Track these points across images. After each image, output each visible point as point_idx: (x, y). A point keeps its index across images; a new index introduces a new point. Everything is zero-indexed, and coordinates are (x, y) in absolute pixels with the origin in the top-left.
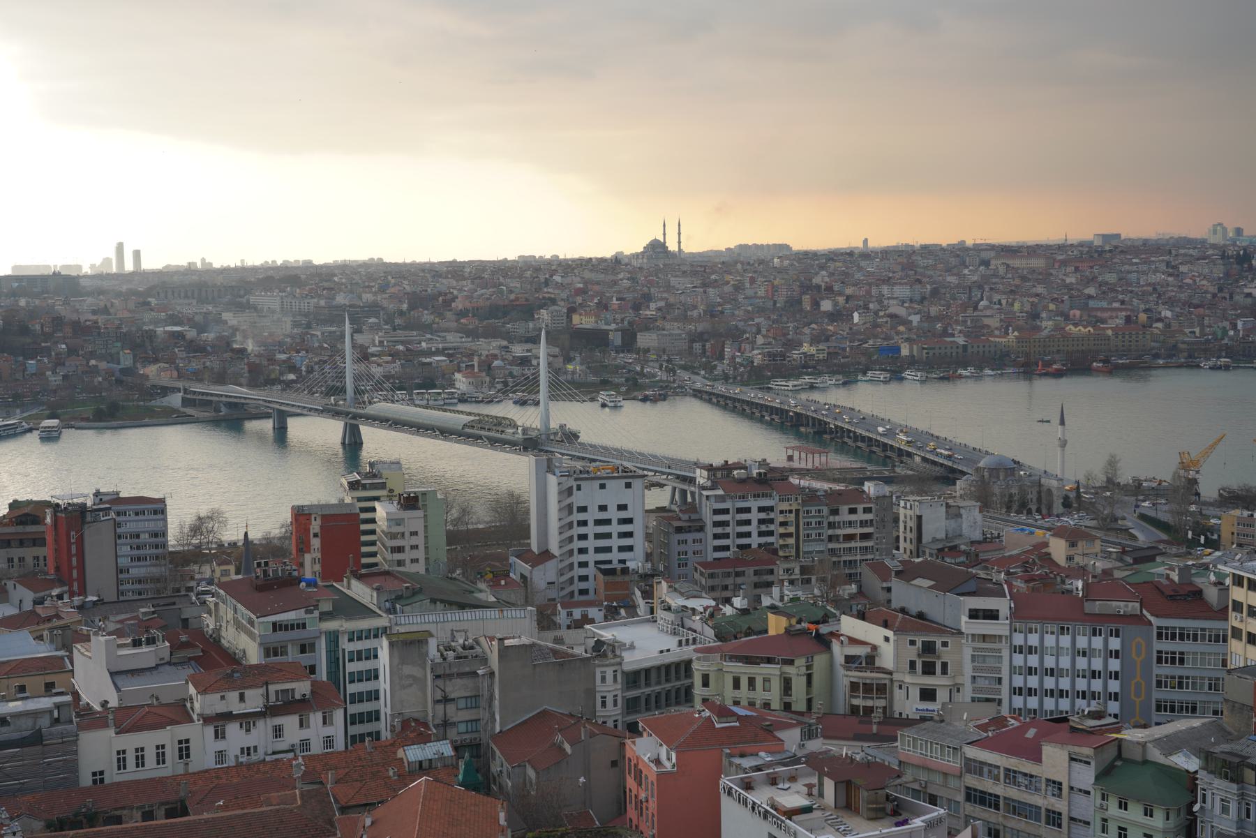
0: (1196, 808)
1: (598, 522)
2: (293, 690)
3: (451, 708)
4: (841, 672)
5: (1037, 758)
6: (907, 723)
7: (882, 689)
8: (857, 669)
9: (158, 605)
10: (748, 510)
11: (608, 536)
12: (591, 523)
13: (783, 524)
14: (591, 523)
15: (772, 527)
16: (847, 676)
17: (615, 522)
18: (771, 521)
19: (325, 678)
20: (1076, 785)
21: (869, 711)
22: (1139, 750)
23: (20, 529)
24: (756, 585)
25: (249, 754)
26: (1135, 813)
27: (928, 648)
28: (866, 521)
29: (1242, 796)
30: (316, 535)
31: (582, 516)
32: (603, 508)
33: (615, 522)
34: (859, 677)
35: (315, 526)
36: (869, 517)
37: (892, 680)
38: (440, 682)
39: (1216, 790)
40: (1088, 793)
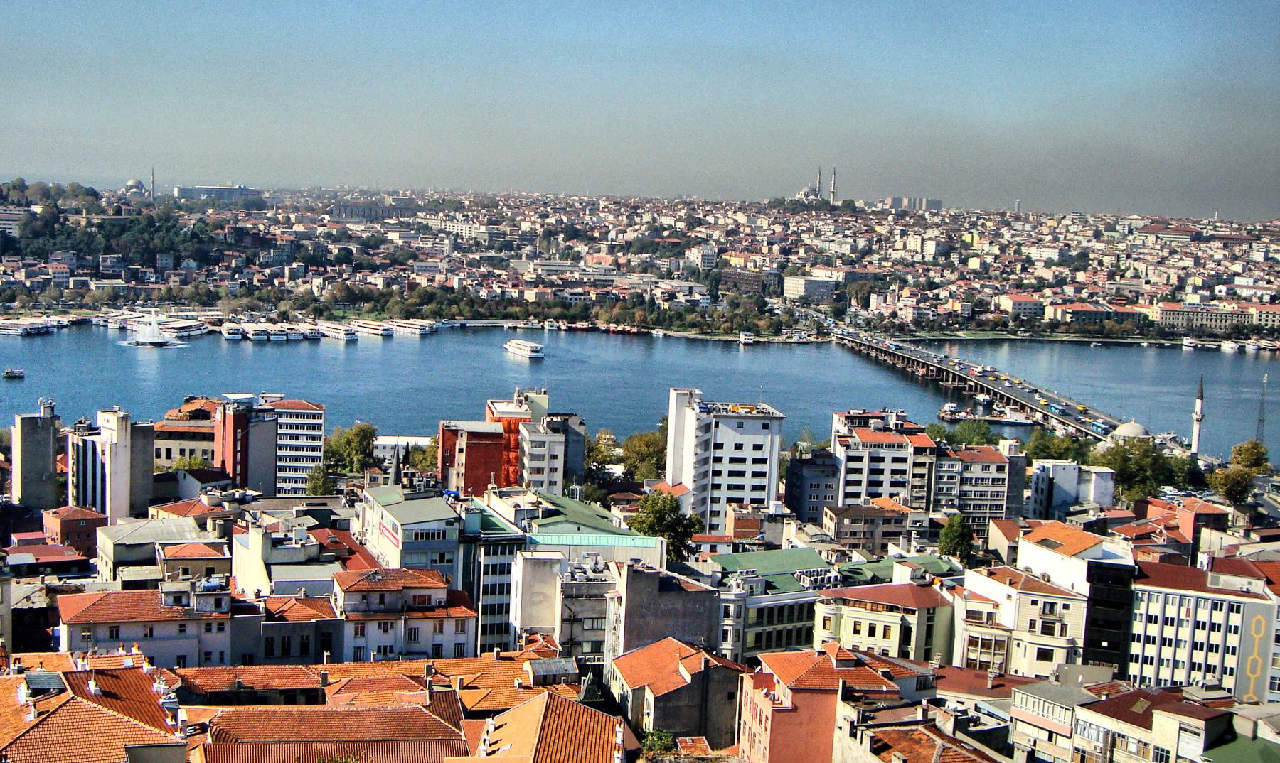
1: (733, 460)
2: (430, 597)
3: (577, 628)
5: (1144, 721)
6: (1022, 682)
7: (999, 644)
8: (980, 625)
9: (311, 505)
11: (742, 474)
12: (726, 460)
14: (726, 460)
16: (966, 630)
17: (749, 461)
19: (460, 588)
21: (985, 666)
22: (1250, 726)
23: (193, 423)
24: (885, 534)
25: (385, 653)
28: (999, 480)
30: (461, 451)
31: (719, 453)
32: (739, 447)
33: (749, 461)
34: (978, 632)
37: (1009, 638)
38: (568, 602)
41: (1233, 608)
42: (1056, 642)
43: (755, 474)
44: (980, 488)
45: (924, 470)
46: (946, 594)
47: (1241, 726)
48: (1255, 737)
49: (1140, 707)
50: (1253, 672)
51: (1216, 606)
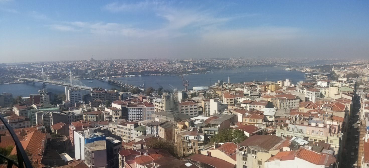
0: (146, 131)
1: (75, 96)
4: (104, 116)
5: (126, 125)
8: (107, 115)
10: (97, 94)
13: (103, 96)
15: (101, 96)
18: (101, 96)
20: (131, 129)
26: (139, 132)
27: (116, 112)
29: (152, 129)
31: (73, 95)
32: (76, 94)
35: (33, 97)
36: (115, 95)
39: (149, 129)
40: (133, 130)
41: (141, 109)
42: (118, 116)
43: (79, 98)
44: (113, 97)
45: (104, 95)
46: (102, 112)
47: (139, 124)
48: (141, 125)
49: (126, 124)
50: (144, 117)
51: (139, 109)
